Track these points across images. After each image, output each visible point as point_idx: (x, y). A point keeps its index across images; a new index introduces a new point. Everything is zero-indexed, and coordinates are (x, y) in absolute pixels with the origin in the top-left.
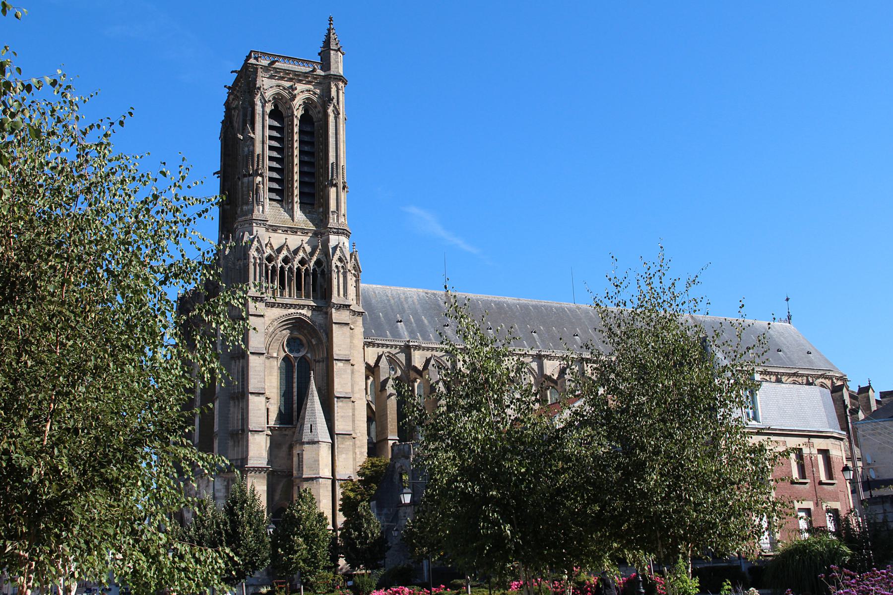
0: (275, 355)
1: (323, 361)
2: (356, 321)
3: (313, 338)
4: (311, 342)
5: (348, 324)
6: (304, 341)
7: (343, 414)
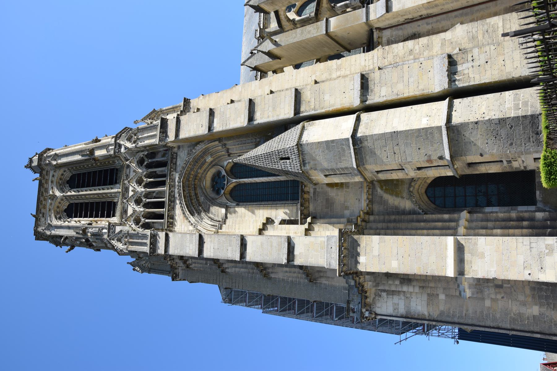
1: (225, 145)
3: (205, 160)
7: (271, 109)
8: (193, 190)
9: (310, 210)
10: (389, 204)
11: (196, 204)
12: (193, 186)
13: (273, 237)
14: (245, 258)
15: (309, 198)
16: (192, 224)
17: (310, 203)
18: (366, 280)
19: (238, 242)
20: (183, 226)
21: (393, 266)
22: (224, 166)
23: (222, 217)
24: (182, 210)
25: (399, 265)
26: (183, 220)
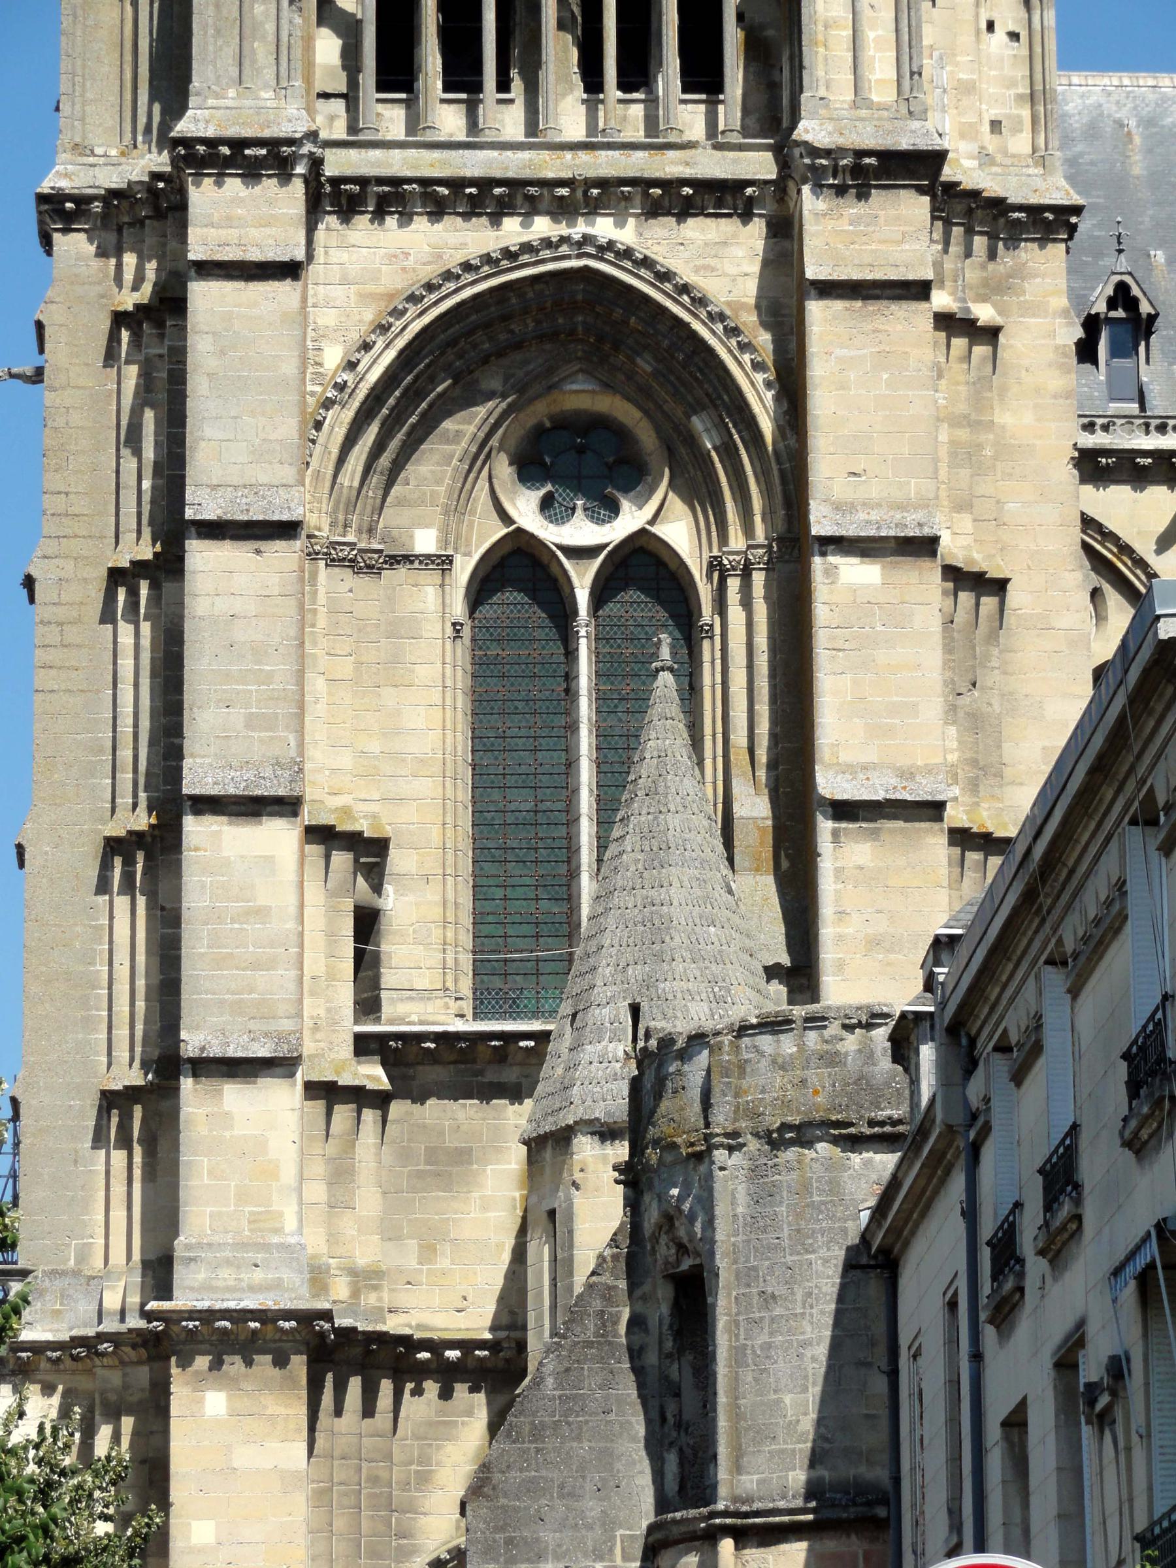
0: (425, 542)
2: (1019, 272)
4: (692, 441)
5: (919, 290)
6: (647, 437)
8: (538, 322)
9: (420, 1068)
10: (439, 1448)
11: (460, 356)
12: (560, 321)
13: (294, 973)
14: (197, 812)
15: (474, 1061)
16: (352, 365)
17: (452, 1067)
18: (129, 1370)
19: (268, 772)
20: (338, 292)
21: (195, 1524)
22: (667, 520)
23: (395, 533)
24: (430, 287)
25: (201, 1550)
26: (371, 296)
